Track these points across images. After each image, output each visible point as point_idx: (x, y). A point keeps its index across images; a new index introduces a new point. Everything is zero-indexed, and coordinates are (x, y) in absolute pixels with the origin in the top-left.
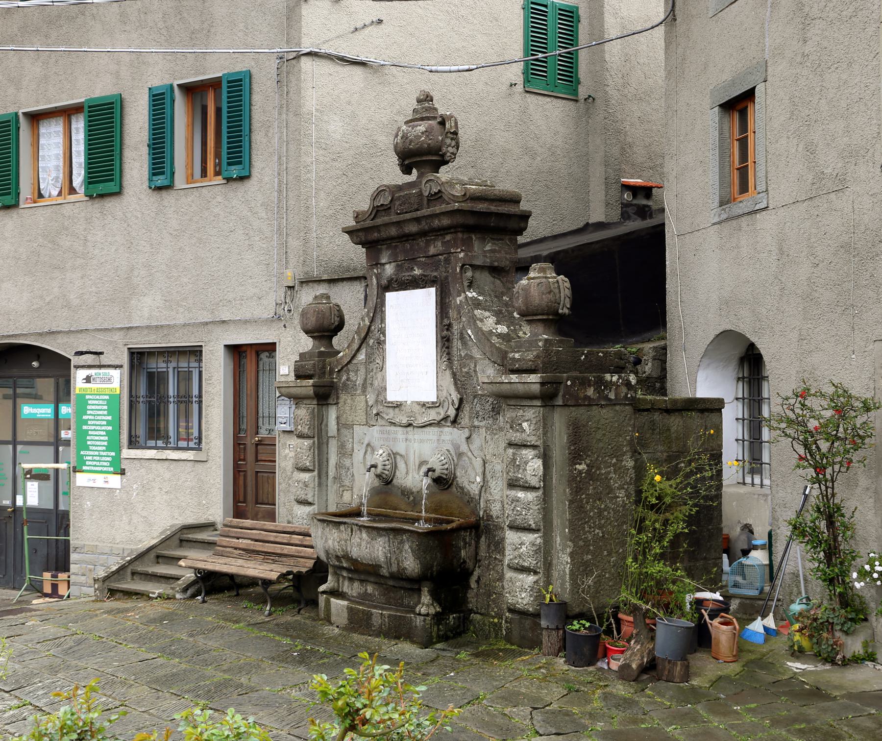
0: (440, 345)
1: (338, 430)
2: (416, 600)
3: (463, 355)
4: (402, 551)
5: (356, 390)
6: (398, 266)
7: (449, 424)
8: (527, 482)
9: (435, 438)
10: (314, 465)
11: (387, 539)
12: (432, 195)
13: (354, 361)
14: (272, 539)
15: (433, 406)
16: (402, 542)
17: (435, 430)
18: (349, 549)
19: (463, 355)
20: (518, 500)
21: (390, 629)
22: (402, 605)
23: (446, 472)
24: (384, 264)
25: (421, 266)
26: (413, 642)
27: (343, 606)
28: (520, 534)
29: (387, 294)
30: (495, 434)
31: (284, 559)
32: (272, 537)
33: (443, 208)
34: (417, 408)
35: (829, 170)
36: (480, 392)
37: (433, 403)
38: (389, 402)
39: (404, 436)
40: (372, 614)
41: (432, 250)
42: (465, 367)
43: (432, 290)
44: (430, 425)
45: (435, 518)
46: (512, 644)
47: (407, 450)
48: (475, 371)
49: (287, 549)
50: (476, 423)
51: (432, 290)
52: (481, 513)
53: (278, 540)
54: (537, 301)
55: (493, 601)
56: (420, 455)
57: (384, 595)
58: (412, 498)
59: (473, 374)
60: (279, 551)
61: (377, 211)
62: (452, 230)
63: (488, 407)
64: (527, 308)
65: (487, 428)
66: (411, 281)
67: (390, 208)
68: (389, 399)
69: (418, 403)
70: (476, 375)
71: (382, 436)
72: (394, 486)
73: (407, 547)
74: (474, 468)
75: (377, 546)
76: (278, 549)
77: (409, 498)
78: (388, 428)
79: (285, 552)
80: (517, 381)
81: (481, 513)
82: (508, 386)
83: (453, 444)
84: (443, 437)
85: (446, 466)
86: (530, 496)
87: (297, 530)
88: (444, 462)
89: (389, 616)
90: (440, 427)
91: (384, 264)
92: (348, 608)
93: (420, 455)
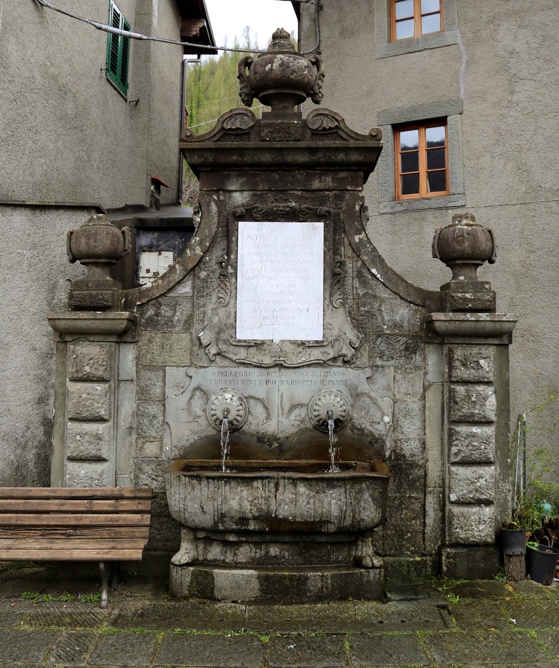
0: (329, 282)
1: (137, 372)
2: (346, 553)
3: (361, 294)
4: (360, 501)
5: (173, 326)
6: (254, 195)
7: (340, 364)
8: (485, 417)
9: (318, 379)
10: (110, 414)
11: (343, 489)
12: (324, 129)
13: (172, 294)
14: (54, 508)
15: (318, 344)
16: (360, 491)
17: (318, 370)
18: (273, 508)
19: (361, 294)
20: (474, 435)
21: (333, 590)
22: (328, 562)
23: (343, 414)
24: (230, 192)
25: (297, 199)
26: (368, 599)
27: (251, 576)
28: (474, 468)
29: (241, 224)
30: (408, 374)
31: (86, 531)
32: (53, 505)
33: (338, 143)
34: (289, 348)
35: (548, 185)
36: (387, 332)
37: (316, 342)
38: (240, 341)
39: (264, 378)
40: (307, 578)
41: (316, 184)
42: (364, 305)
43: (320, 225)
44: (309, 366)
45: (317, 464)
46: (458, 579)
47: (268, 392)
48: (380, 310)
49: (87, 519)
50: (379, 362)
51: (320, 225)
52: (387, 454)
53: (28, 508)
54: (484, 247)
55: (408, 540)
56: (292, 398)
57: (301, 554)
58: (276, 445)
59: (377, 313)
60: (73, 523)
61: (225, 134)
62: (354, 168)
63: (400, 346)
64: (473, 252)
65: (395, 367)
66: (287, 213)
67: (249, 133)
68: (239, 337)
69: (293, 343)
70: (381, 314)
71: (223, 378)
72: (244, 433)
73: (366, 496)
74: (379, 408)
75: (326, 500)
76: (70, 520)
77: (270, 445)
78: (234, 370)
79: (86, 522)
80: (488, 319)
81: (387, 454)
82: (473, 324)
83: (346, 385)
84: (329, 378)
85: (344, 408)
86: (489, 431)
87: (99, 494)
88: (342, 403)
89: (333, 577)
90: (324, 367)
91: (230, 192)
92: (259, 577)
93: (292, 398)
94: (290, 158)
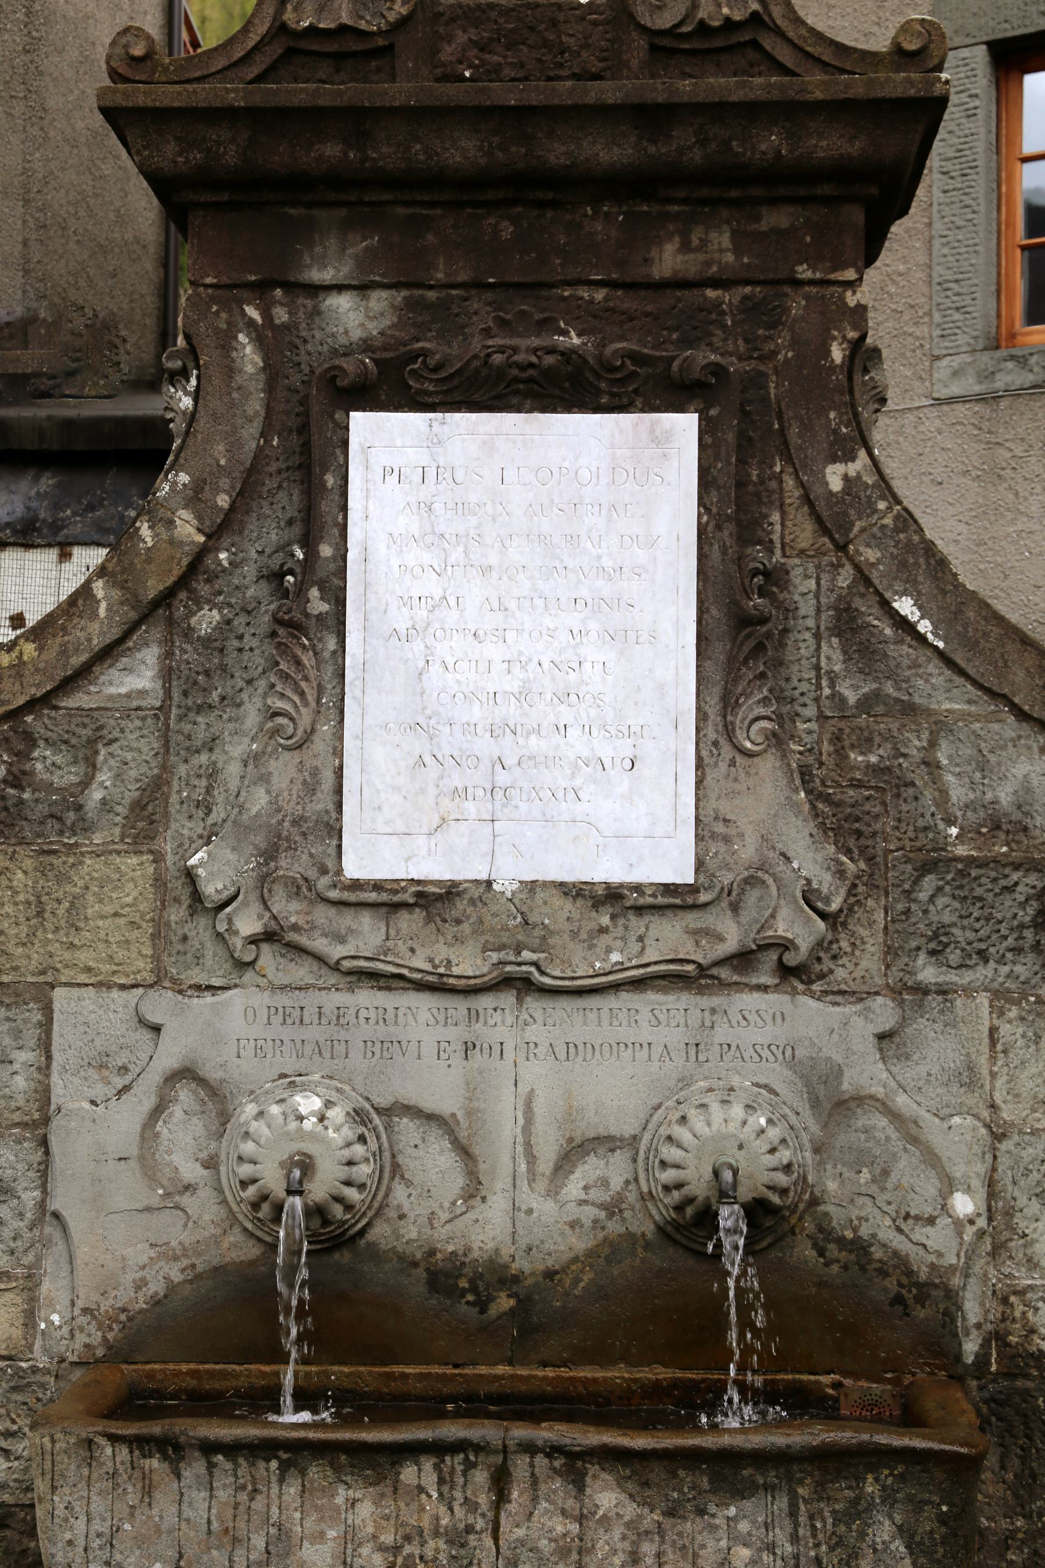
0: (719, 650)
3: (852, 697)
5: (85, 827)
6: (410, 304)
7: (766, 979)
9: (675, 1037)
11: (782, 1503)
12: (703, 28)
15: (674, 900)
16: (857, 1512)
17: (677, 1004)
19: (852, 697)
24: (317, 290)
25: (589, 318)
29: (358, 420)
33: (760, 85)
34: (562, 912)
36: (961, 851)
37: (669, 889)
38: (356, 885)
39: (456, 1034)
41: (668, 260)
42: (866, 743)
43: (683, 428)
44: (638, 984)
45: (675, 1383)
47: (472, 1090)
48: (931, 765)
50: (928, 973)
51: (683, 428)
52: (970, 1347)
56: (570, 1115)
58: (504, 1303)
62: (826, 190)
66: (548, 373)
67: (390, 48)
68: (354, 868)
70: (935, 779)
71: (288, 1033)
72: (374, 1253)
73: (884, 1530)
74: (932, 1159)
77: (482, 1305)
81: (970, 1347)
83: (792, 1063)
84: (722, 1033)
85: (785, 1155)
88: (774, 1134)
90: (701, 991)
91: (317, 290)
93: (570, 1115)
94: (557, 152)
